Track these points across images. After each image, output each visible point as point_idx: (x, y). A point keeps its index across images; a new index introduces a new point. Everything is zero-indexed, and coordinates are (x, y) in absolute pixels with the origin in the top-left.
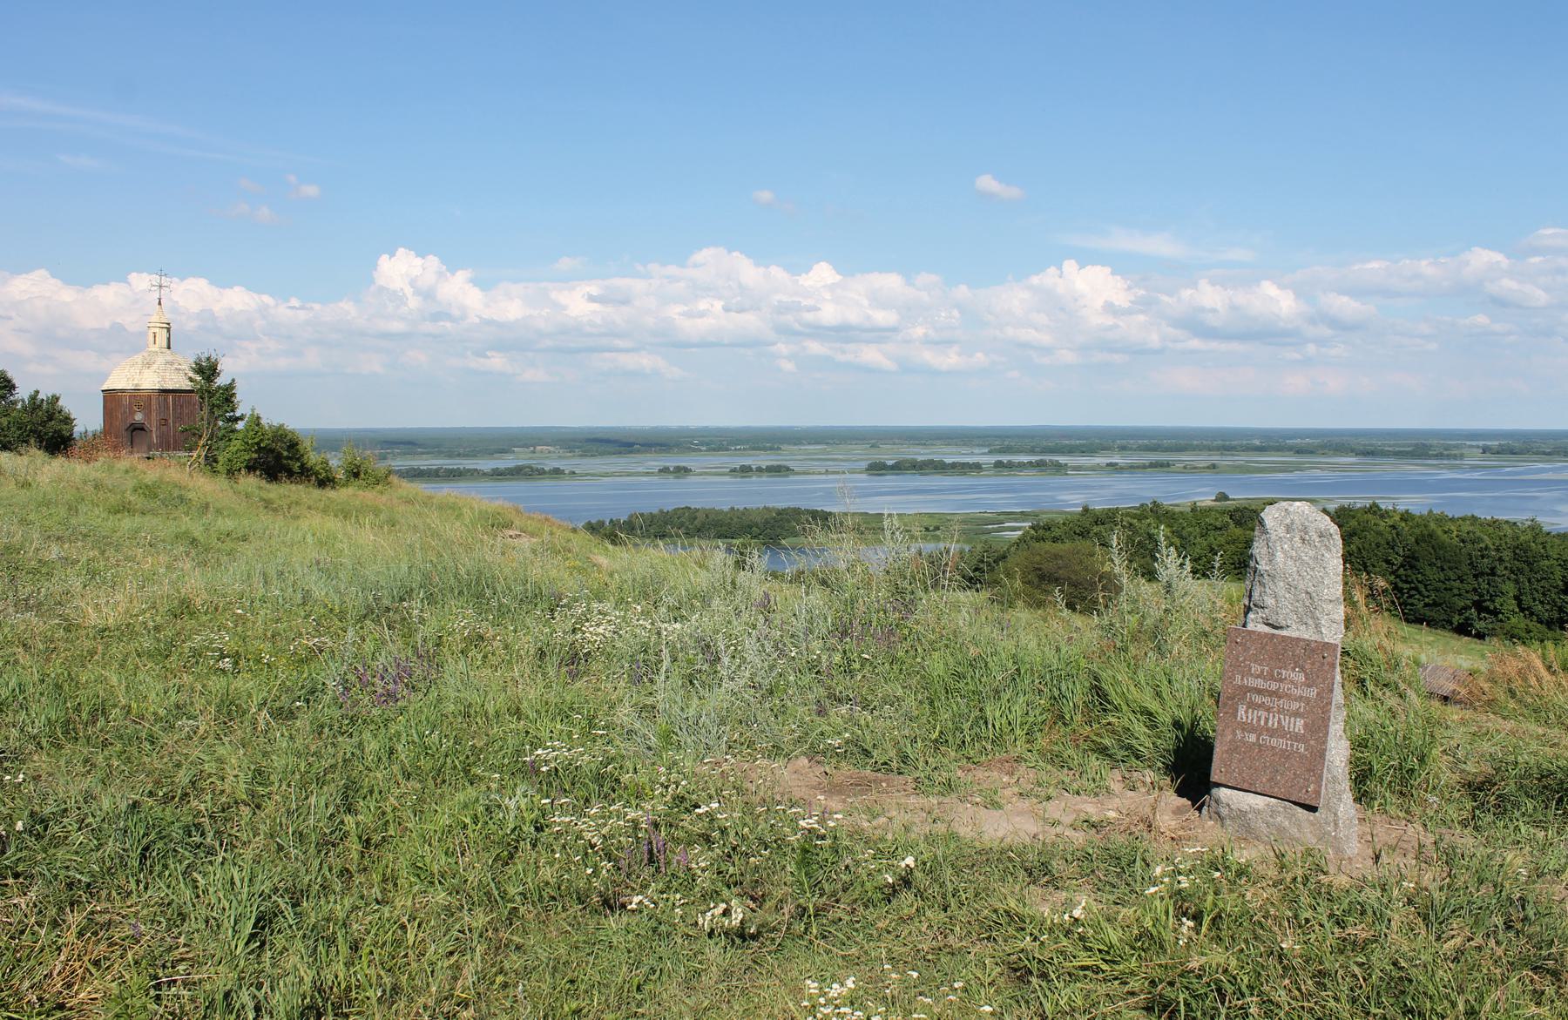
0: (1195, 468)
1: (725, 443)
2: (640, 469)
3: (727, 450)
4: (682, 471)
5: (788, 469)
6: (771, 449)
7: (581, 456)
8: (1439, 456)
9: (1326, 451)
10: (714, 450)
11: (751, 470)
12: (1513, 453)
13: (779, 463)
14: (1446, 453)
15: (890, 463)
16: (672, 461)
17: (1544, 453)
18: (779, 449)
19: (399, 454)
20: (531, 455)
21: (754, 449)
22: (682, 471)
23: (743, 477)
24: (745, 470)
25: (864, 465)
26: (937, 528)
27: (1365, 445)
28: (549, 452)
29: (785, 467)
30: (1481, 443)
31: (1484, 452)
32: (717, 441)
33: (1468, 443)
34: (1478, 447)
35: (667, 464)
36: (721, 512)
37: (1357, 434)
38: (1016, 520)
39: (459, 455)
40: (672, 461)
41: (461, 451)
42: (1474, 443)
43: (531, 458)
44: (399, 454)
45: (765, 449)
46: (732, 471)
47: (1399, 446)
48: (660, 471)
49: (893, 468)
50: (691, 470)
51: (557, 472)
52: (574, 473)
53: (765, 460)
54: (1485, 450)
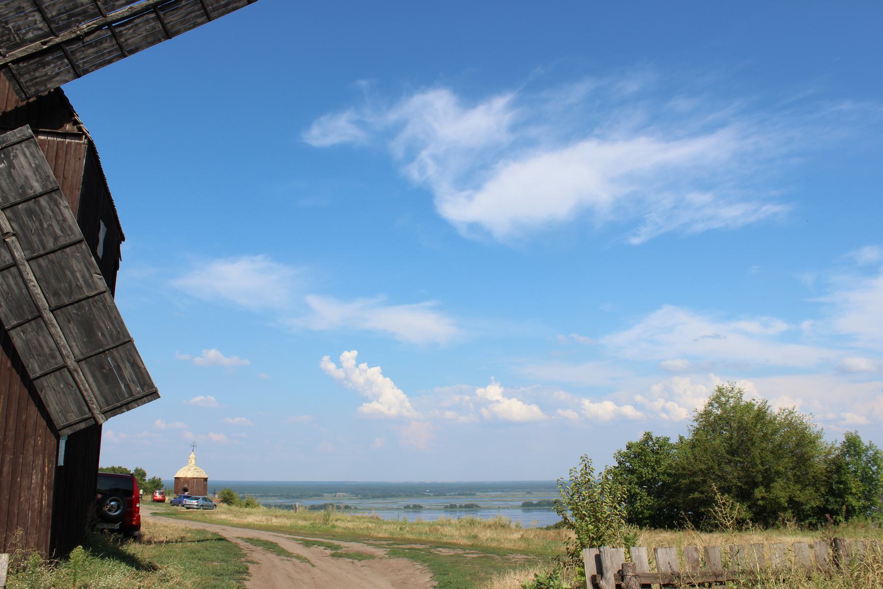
1: (444, 491)
2: (395, 506)
3: (445, 495)
4: (417, 508)
5: (477, 506)
6: (470, 495)
7: (361, 499)
10: (437, 495)
11: (455, 506)
13: (472, 503)
15: (535, 502)
16: (412, 502)
18: (474, 494)
19: (259, 496)
20: (334, 498)
21: (460, 495)
23: (451, 511)
24: (453, 507)
25: (521, 503)
28: (344, 496)
29: (475, 505)
32: (439, 490)
39: (293, 497)
40: (412, 502)
41: (294, 495)
43: (333, 500)
44: (259, 496)
45: (466, 495)
46: (446, 507)
49: (536, 505)
50: (422, 507)
51: (347, 507)
52: (357, 508)
53: (465, 501)
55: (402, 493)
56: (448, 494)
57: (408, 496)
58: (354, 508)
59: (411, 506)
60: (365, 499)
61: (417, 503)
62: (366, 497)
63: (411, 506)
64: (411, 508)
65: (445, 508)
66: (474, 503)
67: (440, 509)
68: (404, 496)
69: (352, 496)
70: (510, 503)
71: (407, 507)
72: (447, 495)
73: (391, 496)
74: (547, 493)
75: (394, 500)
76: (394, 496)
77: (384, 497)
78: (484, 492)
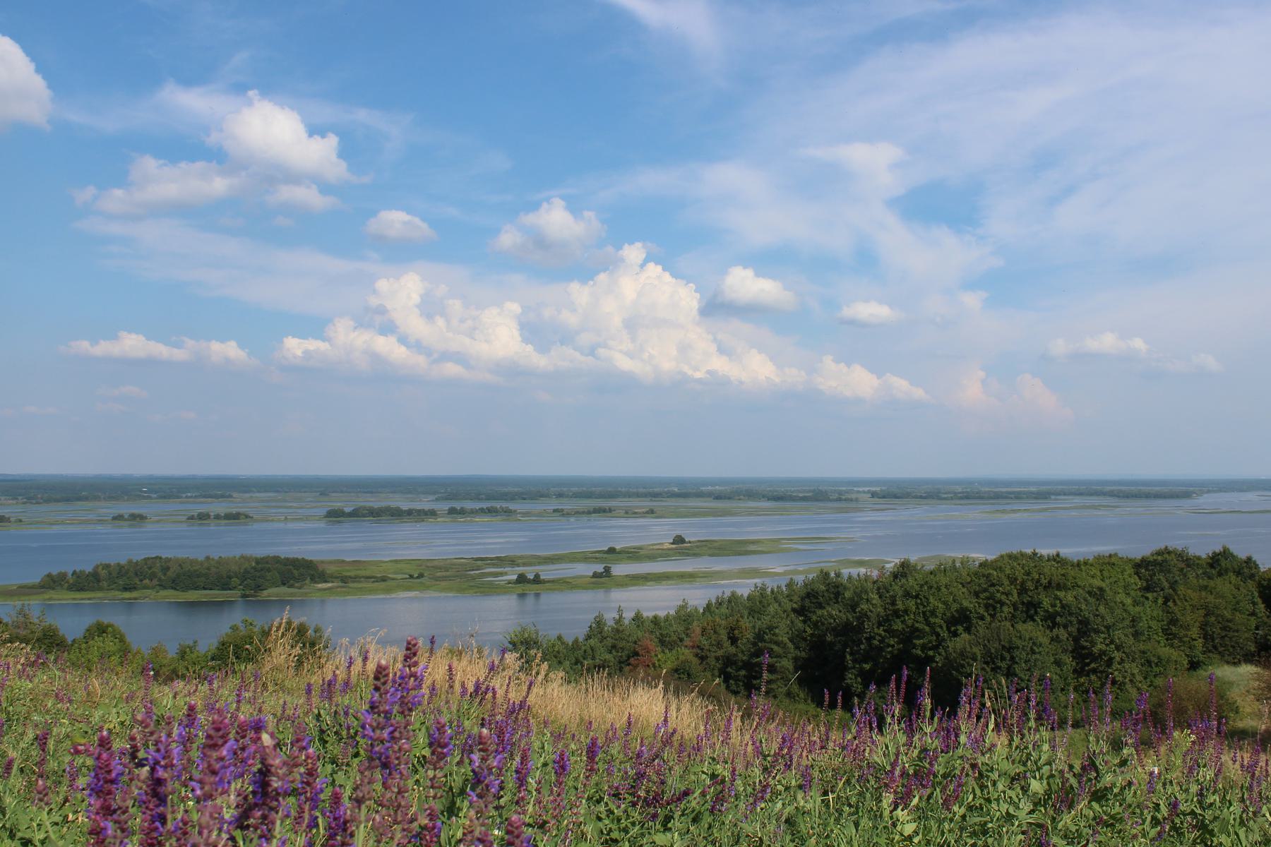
0: (636, 513)
2: (91, 517)
4: (138, 518)
8: (839, 500)
9: (742, 497)
12: (896, 497)
14: (844, 497)
16: (126, 508)
17: (921, 497)
22: (138, 518)
23: (200, 524)
26: (421, 576)
27: (770, 491)
30: (866, 489)
31: (873, 497)
33: (855, 489)
34: (864, 492)
35: (121, 512)
36: (193, 562)
37: (705, 482)
38: (494, 565)
40: (126, 508)
42: (861, 489)
47: (799, 491)
48: (115, 518)
50: (146, 518)
54: (874, 495)
55: (100, 494)
56: (184, 495)
57: (111, 498)
58: (16, 522)
59: (126, 517)
60: (31, 503)
61: (137, 511)
62: (34, 501)
63: (126, 517)
64: (126, 520)
65: (188, 519)
66: (241, 510)
67: (181, 522)
68: (104, 499)
69: (6, 499)
70: (300, 511)
71: (119, 518)
72: (181, 497)
73: (79, 499)
74: (352, 494)
75: (89, 504)
76: (86, 499)
77: (68, 500)
78: (245, 492)
